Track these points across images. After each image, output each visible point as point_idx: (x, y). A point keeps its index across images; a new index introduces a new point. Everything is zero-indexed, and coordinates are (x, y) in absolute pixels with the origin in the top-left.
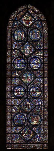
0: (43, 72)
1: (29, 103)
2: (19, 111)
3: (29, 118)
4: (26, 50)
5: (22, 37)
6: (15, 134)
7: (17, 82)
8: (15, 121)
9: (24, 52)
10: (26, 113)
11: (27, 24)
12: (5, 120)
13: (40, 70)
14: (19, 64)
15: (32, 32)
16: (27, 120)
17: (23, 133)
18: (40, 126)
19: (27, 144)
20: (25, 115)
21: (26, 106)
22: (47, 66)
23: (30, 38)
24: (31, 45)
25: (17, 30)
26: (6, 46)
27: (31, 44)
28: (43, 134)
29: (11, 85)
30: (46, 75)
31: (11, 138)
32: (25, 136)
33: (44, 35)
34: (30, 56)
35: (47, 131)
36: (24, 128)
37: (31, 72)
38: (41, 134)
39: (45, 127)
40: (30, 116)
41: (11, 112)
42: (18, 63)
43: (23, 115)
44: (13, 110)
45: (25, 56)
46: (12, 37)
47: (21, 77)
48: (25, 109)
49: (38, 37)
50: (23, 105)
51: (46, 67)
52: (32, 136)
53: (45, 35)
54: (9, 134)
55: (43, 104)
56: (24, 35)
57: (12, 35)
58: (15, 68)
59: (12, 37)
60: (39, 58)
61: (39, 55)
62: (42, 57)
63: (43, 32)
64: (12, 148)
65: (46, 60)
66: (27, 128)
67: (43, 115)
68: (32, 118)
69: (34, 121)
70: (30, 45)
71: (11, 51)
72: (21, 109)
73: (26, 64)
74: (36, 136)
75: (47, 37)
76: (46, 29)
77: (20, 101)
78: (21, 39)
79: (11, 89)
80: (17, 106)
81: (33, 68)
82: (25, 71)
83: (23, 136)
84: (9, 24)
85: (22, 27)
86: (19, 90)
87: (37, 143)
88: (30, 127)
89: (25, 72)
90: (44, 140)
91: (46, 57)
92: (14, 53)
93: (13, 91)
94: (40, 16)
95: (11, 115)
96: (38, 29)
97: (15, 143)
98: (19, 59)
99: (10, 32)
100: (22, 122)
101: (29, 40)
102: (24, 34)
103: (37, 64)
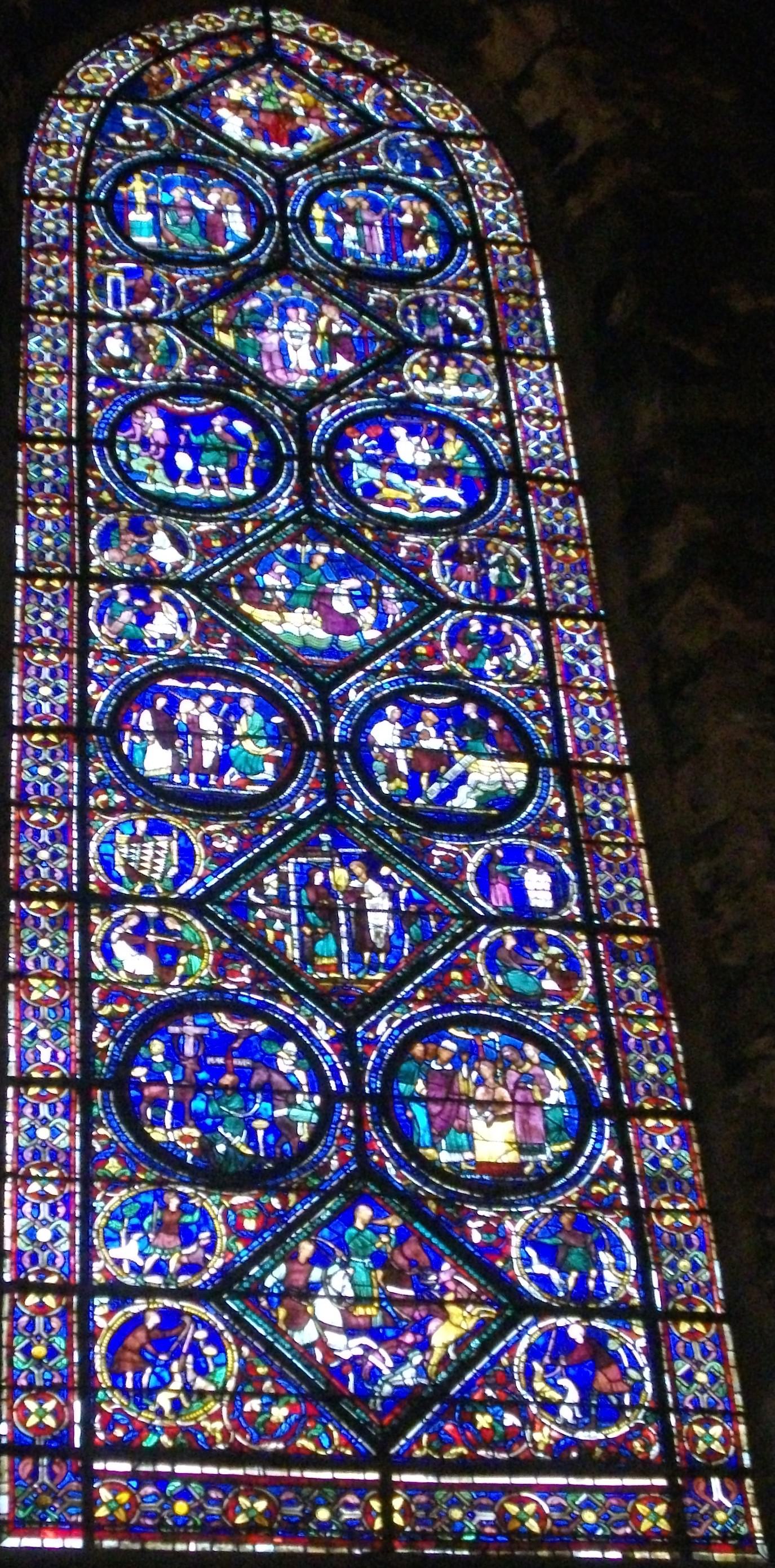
0: (532, 556)
1: (373, 872)
2: (221, 966)
3: (390, 1071)
6: (148, 1292)
7: (164, 623)
10: (321, 998)
11: (268, 141)
16: (356, 1097)
18: (585, 1192)
21: (329, 914)
29: (83, 652)
30: (571, 591)
32: (337, 1341)
33: (481, 243)
38: (621, 1313)
39: (660, 1212)
40: (403, 1050)
41: (78, 979)
44: (122, 950)
47: (223, 585)
48: (308, 957)
50: (282, 900)
52: (461, 1343)
54: (42, 1289)
55: (584, 903)
62: (489, 413)
66: (364, 1213)
68: (429, 1077)
69: (478, 1125)
70: (320, 299)
72: (241, 942)
74: (532, 1332)
77: (230, 844)
78: (209, 248)
79: (86, 703)
80: (184, 903)
82: (281, 526)
83: (306, 1335)
84: (46, 122)
86: (208, 723)
90: (682, 1412)
93: (120, 719)
94: (421, 102)
95: (90, 1018)
97: (158, 1454)
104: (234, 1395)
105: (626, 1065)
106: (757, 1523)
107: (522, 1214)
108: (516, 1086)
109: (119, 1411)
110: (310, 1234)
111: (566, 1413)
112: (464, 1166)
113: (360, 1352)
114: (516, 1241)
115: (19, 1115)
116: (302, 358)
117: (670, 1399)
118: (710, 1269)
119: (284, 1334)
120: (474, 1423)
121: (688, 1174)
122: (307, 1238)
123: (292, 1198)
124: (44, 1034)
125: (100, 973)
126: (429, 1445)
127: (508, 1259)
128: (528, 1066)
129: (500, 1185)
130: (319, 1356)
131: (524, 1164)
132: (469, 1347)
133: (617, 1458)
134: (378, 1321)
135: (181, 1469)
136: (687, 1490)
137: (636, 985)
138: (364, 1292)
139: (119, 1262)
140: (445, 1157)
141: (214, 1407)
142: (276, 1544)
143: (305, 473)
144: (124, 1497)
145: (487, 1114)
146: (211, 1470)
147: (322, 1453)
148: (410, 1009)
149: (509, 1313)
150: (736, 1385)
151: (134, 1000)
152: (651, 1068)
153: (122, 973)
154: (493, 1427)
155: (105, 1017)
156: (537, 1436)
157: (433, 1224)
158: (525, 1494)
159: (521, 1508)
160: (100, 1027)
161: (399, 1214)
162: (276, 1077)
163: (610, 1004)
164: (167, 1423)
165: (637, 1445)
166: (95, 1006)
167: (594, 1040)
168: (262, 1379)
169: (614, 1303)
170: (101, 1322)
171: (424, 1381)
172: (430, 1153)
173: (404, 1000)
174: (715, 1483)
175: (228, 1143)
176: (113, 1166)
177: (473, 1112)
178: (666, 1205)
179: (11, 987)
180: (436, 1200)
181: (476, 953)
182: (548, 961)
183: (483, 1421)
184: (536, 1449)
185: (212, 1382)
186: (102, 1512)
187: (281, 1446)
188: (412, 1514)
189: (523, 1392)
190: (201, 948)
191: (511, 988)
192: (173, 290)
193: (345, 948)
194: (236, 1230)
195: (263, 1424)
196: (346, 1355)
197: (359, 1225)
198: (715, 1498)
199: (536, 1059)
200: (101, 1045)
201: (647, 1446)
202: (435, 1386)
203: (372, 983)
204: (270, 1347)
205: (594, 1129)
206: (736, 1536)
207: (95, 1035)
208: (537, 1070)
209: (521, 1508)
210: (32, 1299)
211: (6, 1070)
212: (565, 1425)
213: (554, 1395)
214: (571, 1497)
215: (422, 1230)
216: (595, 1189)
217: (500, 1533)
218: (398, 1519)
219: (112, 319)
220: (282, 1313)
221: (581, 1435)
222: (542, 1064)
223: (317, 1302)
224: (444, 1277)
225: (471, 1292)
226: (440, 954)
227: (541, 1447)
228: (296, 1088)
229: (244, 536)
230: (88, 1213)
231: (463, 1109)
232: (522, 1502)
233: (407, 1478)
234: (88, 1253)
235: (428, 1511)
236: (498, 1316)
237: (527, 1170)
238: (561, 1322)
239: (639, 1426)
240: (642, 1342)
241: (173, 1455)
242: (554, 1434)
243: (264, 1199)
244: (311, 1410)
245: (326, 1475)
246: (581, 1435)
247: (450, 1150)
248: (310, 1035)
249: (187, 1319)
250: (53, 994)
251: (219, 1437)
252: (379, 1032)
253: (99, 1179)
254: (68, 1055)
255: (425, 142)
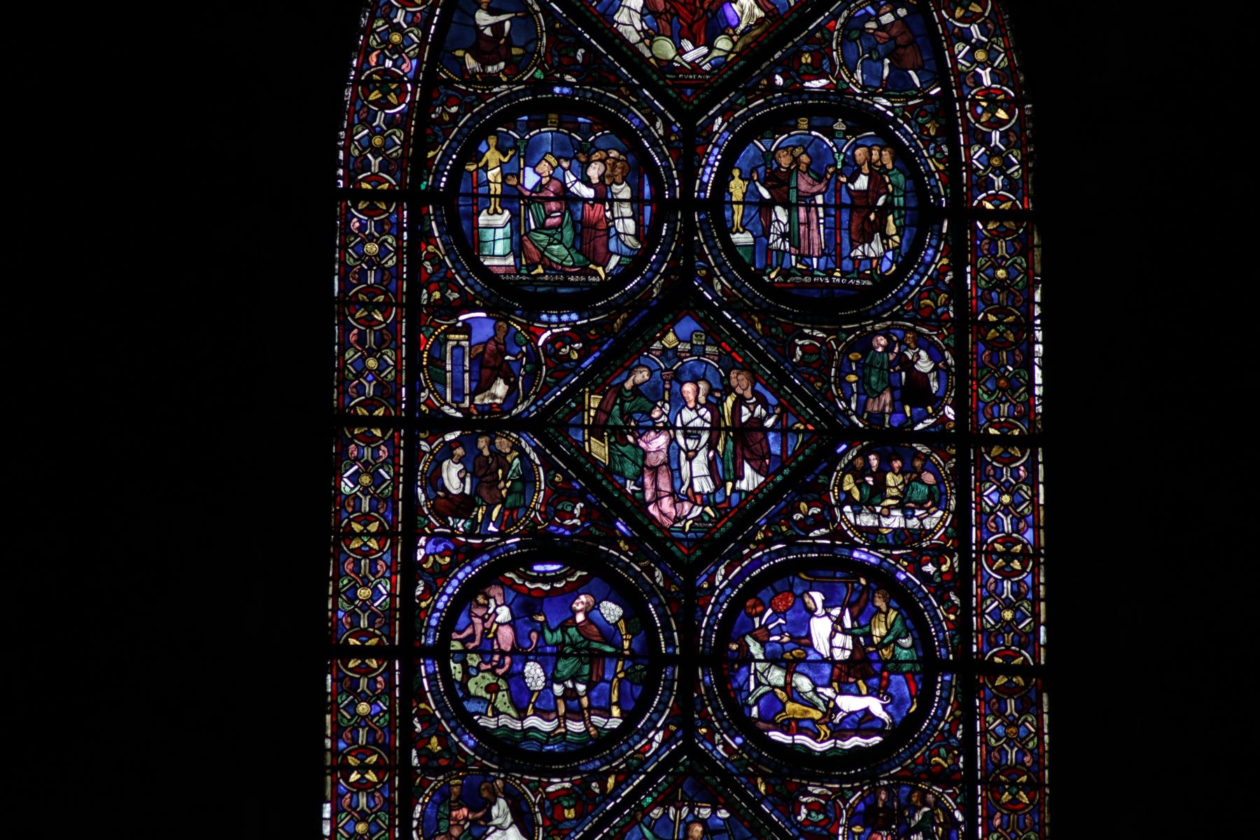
4: (661, 441)
5: (591, 238)
9: (630, 469)
13: (911, 777)
14: (539, 656)
15: (769, 156)
22: (1028, 705)
23: (730, 247)
24: (746, 367)
25: (508, 118)
26: (321, 368)
27: (745, 343)
33: (964, 215)
34: (730, 536)
37: (754, 804)
42: (520, 653)
45: (653, 540)
46: (420, 235)
49: (875, 248)
51: (1015, 733)
53: (986, 216)
56: (636, 200)
57: (433, 193)
58: (466, 721)
59: (429, 237)
60: (881, 578)
61: (895, 520)
63: (954, 163)
65: (1010, 602)
70: (727, 363)
71: (414, 454)
73: (670, 660)
75: (1026, 251)
76: (996, 124)
81: (776, 736)
84: (369, 31)
85: (593, 71)
89: (641, 789)
91: (1008, 556)
92: (453, 477)
96: (864, 120)
98: (544, 578)
99: (395, 152)
101: (708, 282)
102: (624, 192)
103: (860, 669)
116: (698, 473)
143: (689, 682)
192: (533, 355)
219: (452, 424)
229: (606, 796)
255: (902, 12)
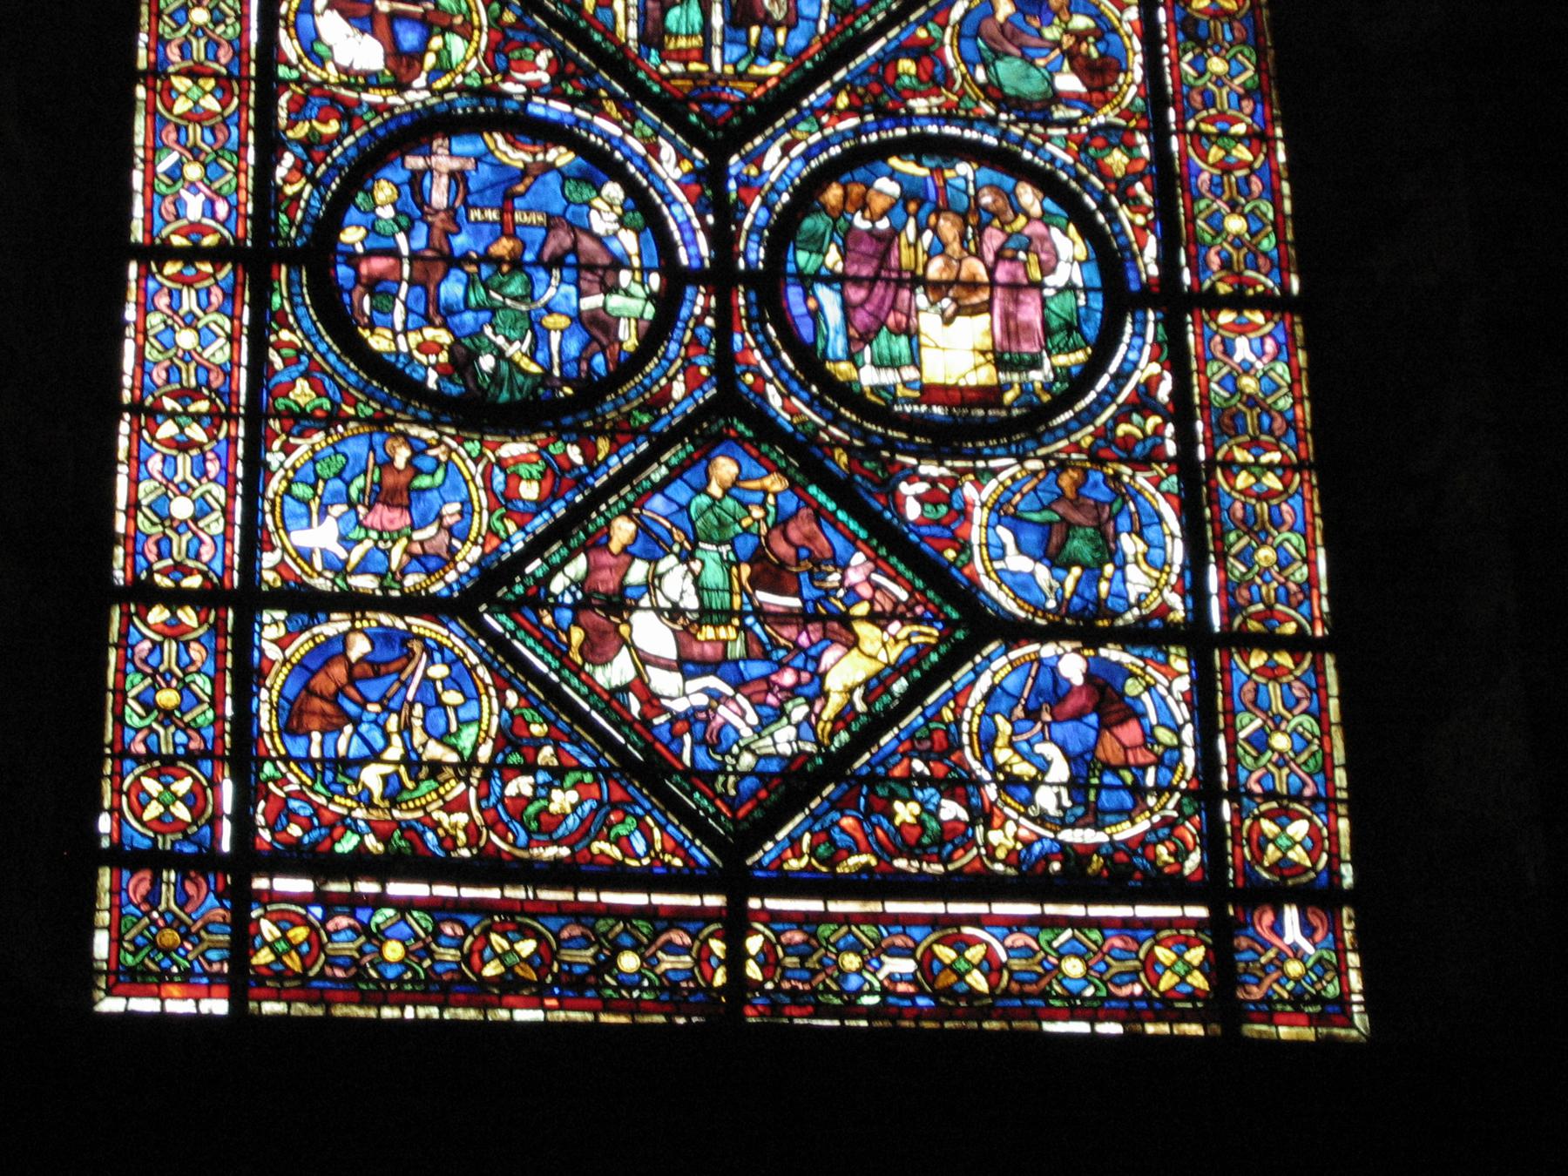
2: (501, 53)
6: (354, 603)
8: (374, 285)
10: (671, 108)
12: (92, 253)
17: (609, 606)
19: (737, 879)
20: (670, 167)
28: (1194, 636)
31: (245, 717)
32: (664, 682)
35: (1290, 561)
36: (642, 463)
38: (1151, 634)
39: (1230, 466)
40: (807, 194)
41: (259, 78)
43: (601, 164)
48: (654, 34)
52: (875, 686)
54: (176, 598)
64: (279, 981)
66: (725, 468)
67: (1166, 177)
69: (929, 322)
74: (998, 666)
83: (618, 671)
87: (1028, 879)
88: (803, 456)
100: (578, 318)
104: (488, 770)
105: (1191, 219)
106: (1355, 980)
107: (994, 473)
108: (999, 255)
109: (300, 795)
110: (630, 505)
111: (1046, 799)
112: (901, 391)
113: (702, 700)
114: (979, 516)
115: (145, 308)
117: (1225, 777)
118: (1309, 561)
119: (577, 671)
120: (891, 816)
121: (1285, 403)
122: (627, 513)
123: (603, 445)
124: (193, 171)
125: (291, 66)
126: (813, 853)
127: (964, 547)
128: (1022, 220)
129: (964, 426)
130: (635, 707)
131: (1001, 389)
132: (888, 691)
133: (1126, 876)
134: (737, 650)
135: (396, 889)
136: (1242, 925)
137: (1219, 81)
138: (717, 601)
139: (305, 556)
140: (869, 377)
141: (456, 789)
142: (546, 1009)
144: (299, 934)
145: (946, 302)
146: (445, 891)
147: (633, 863)
148: (822, 127)
149: (960, 635)
150: (1339, 755)
151: (348, 114)
152: (1235, 224)
153: (330, 66)
154: (920, 822)
155: (299, 142)
156: (995, 837)
157: (841, 490)
158: (967, 930)
159: (960, 953)
160: (288, 159)
161: (783, 472)
162: (586, 243)
163: (1172, 114)
164: (375, 815)
165: (1162, 851)
166: (283, 122)
167: (1140, 176)
168: (538, 744)
169: (1143, 619)
170: (273, 652)
171: (810, 747)
172: (843, 370)
173: (815, 111)
174: (1291, 914)
175: (500, 354)
176: (302, 393)
177: (921, 300)
178: (1241, 455)
179: (141, 92)
180: (848, 448)
181: (943, 28)
182: (1068, 42)
183: (905, 812)
184: (994, 859)
185: (454, 748)
186: (264, 957)
187: (565, 852)
188: (778, 962)
189: (976, 765)
190: (468, 22)
191: (1000, 87)
193: (717, 20)
194: (505, 502)
195: (537, 817)
196: (680, 706)
197: (715, 490)
198: (1288, 940)
199: (1036, 210)
200: (290, 190)
201: (1180, 854)
202: (827, 756)
203: (761, 80)
204: (553, 693)
205: (1128, 329)
206: (1318, 999)
207: (281, 172)
208: (1038, 228)
209: (960, 953)
210: (158, 615)
211: (128, 231)
212: (1042, 819)
213: (1024, 769)
214: (1045, 936)
215: (822, 498)
216: (1122, 429)
217: (921, 992)
218: (753, 971)
220: (577, 635)
221: (1067, 835)
222: (1046, 218)
223: (637, 618)
224: (854, 577)
225: (897, 603)
226: (880, 30)
227: (1001, 854)
228: (618, 263)
230: (257, 470)
231: (905, 294)
232: (960, 944)
233: (773, 904)
234: (254, 540)
235: (804, 958)
236: (941, 640)
237: (1009, 397)
238: (1048, 650)
239: (1168, 823)
240: (1182, 684)
241: (383, 868)
242: (1023, 833)
243: (556, 449)
244: (618, 794)
245: (638, 899)
246: (1067, 835)
247: (879, 364)
248: (648, 171)
249: (416, 646)
250: (211, 103)
251: (462, 837)
252: (766, 166)
253: (278, 415)
254: (232, 208)
